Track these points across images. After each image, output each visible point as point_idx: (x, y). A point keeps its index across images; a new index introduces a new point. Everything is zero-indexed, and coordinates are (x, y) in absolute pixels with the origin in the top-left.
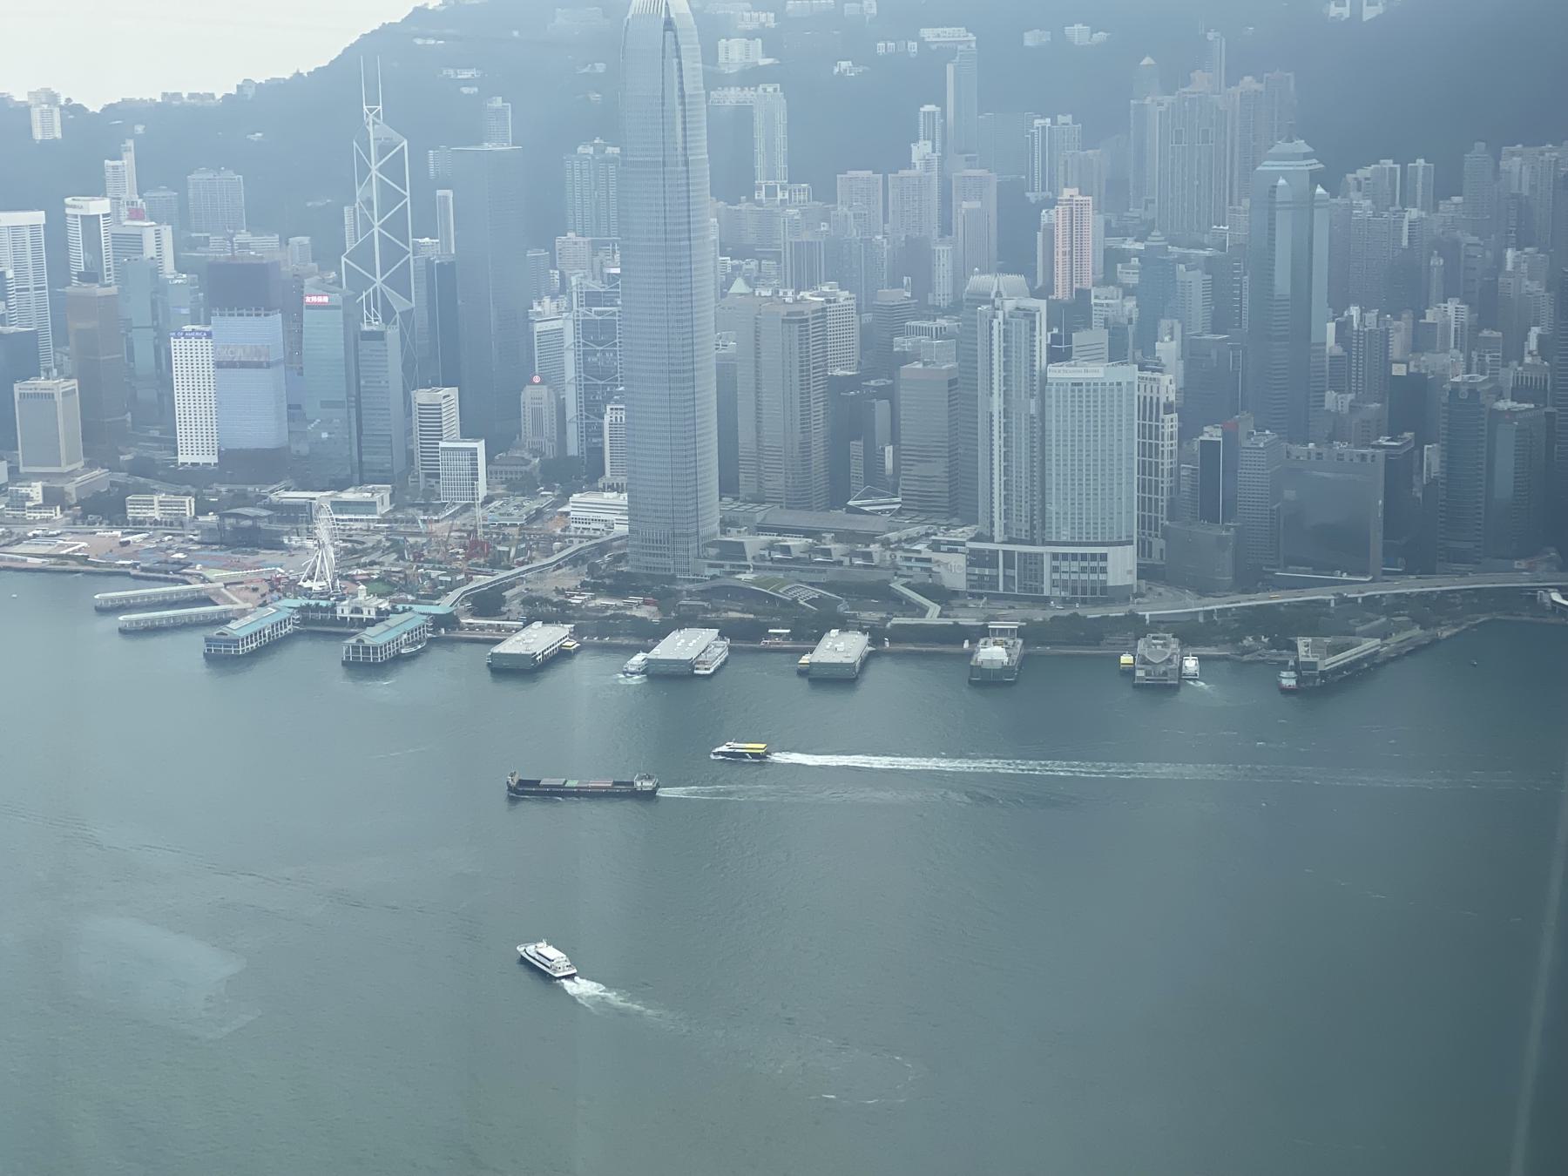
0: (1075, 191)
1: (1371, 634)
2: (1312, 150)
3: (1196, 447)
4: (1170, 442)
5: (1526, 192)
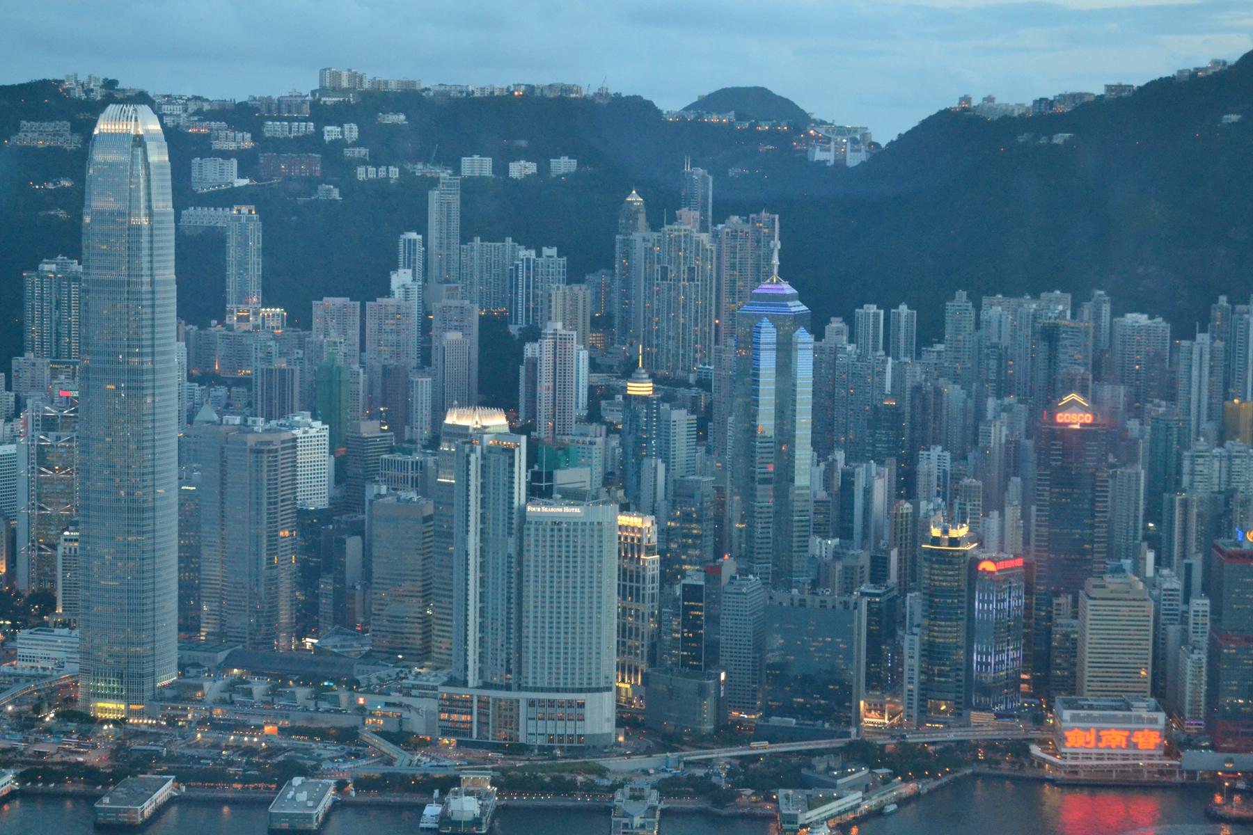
0: (559, 325)
1: (853, 787)
2: (795, 291)
3: (678, 591)
4: (651, 585)
5: (1006, 341)
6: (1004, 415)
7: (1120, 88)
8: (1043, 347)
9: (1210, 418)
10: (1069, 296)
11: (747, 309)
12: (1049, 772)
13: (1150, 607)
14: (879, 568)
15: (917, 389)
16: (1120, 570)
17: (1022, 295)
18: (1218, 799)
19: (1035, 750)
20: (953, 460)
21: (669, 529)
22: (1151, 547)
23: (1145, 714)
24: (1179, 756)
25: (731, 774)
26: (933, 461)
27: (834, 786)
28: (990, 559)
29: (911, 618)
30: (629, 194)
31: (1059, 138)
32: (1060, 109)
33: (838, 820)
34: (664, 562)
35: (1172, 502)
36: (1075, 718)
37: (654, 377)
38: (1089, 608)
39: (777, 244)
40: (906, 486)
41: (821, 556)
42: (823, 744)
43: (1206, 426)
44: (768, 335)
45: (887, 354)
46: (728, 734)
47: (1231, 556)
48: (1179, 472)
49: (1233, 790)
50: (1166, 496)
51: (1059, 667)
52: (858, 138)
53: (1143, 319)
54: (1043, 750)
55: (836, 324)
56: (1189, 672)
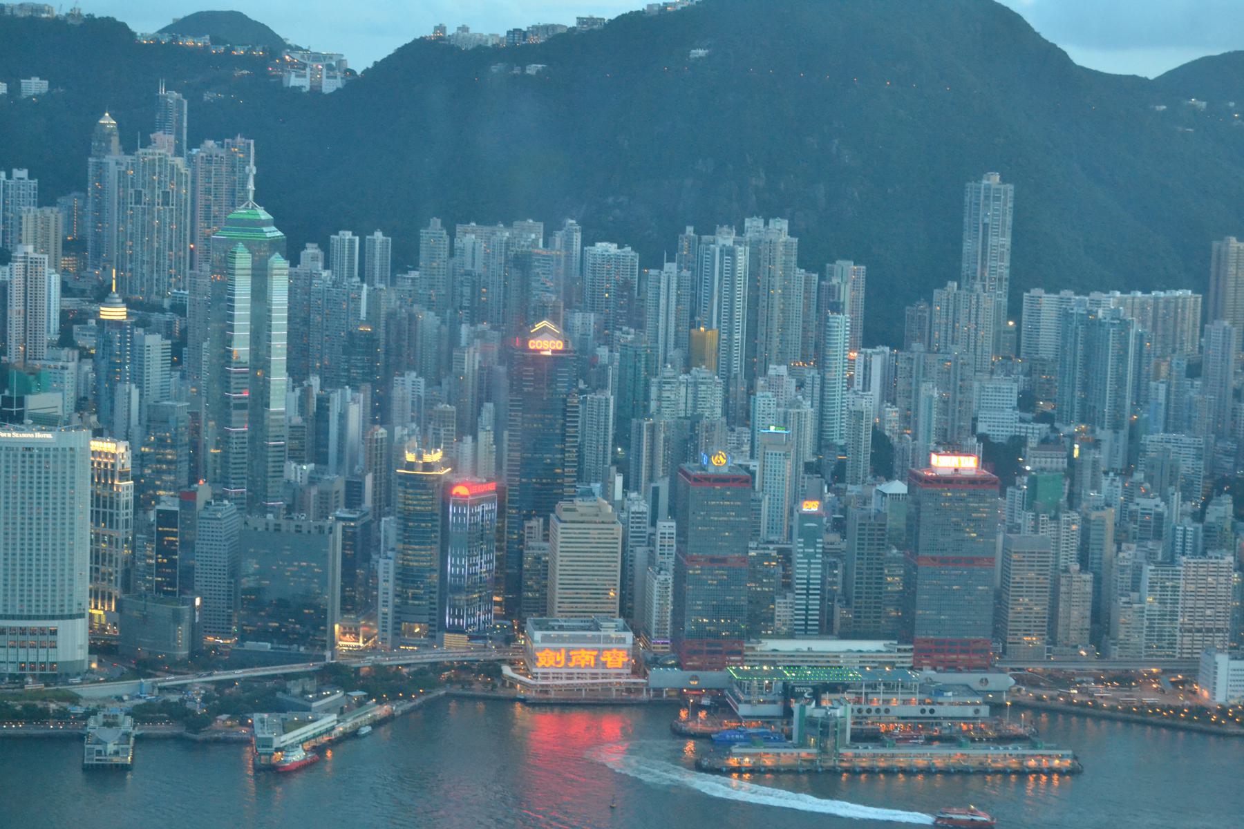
0: (30, 249)
1: (328, 711)
2: (269, 217)
3: (152, 517)
4: (125, 511)
5: (479, 268)
6: (478, 342)
7: (592, 21)
8: (516, 274)
9: (677, 345)
10: (541, 225)
11: (221, 235)
12: (520, 692)
13: (618, 529)
14: (353, 494)
15: (391, 315)
16: (590, 493)
17: (494, 223)
18: (683, 714)
19: (507, 670)
20: (428, 385)
21: (143, 455)
22: (619, 471)
23: (613, 634)
24: (646, 674)
25: (205, 699)
26: (408, 386)
27: (308, 709)
28: (463, 484)
29: (386, 542)
30: (102, 116)
31: (532, 69)
32: (533, 40)
33: (313, 743)
34: (138, 488)
35: (640, 427)
36: (545, 639)
37: (129, 303)
38: (559, 529)
39: (252, 169)
40: (380, 411)
41: (296, 482)
42: (298, 668)
43: (672, 353)
44: (243, 260)
45: (362, 281)
46: (201, 659)
47: (698, 480)
48: (647, 398)
49: (698, 707)
50: (634, 421)
51: (530, 589)
52: (334, 65)
53: (612, 248)
54: (514, 670)
55: (311, 250)
56: (655, 593)
